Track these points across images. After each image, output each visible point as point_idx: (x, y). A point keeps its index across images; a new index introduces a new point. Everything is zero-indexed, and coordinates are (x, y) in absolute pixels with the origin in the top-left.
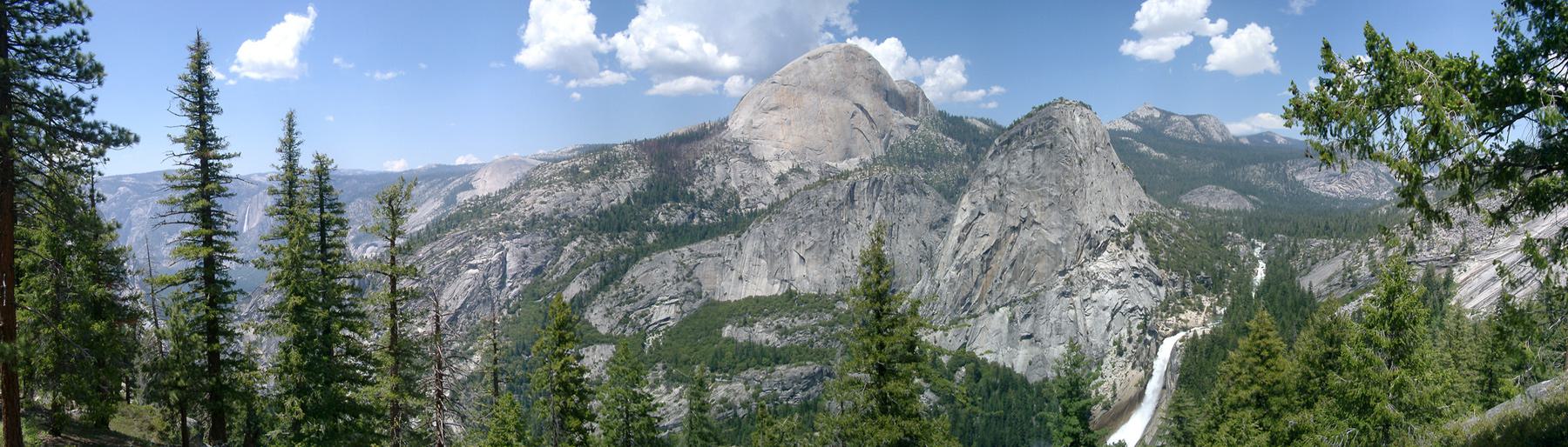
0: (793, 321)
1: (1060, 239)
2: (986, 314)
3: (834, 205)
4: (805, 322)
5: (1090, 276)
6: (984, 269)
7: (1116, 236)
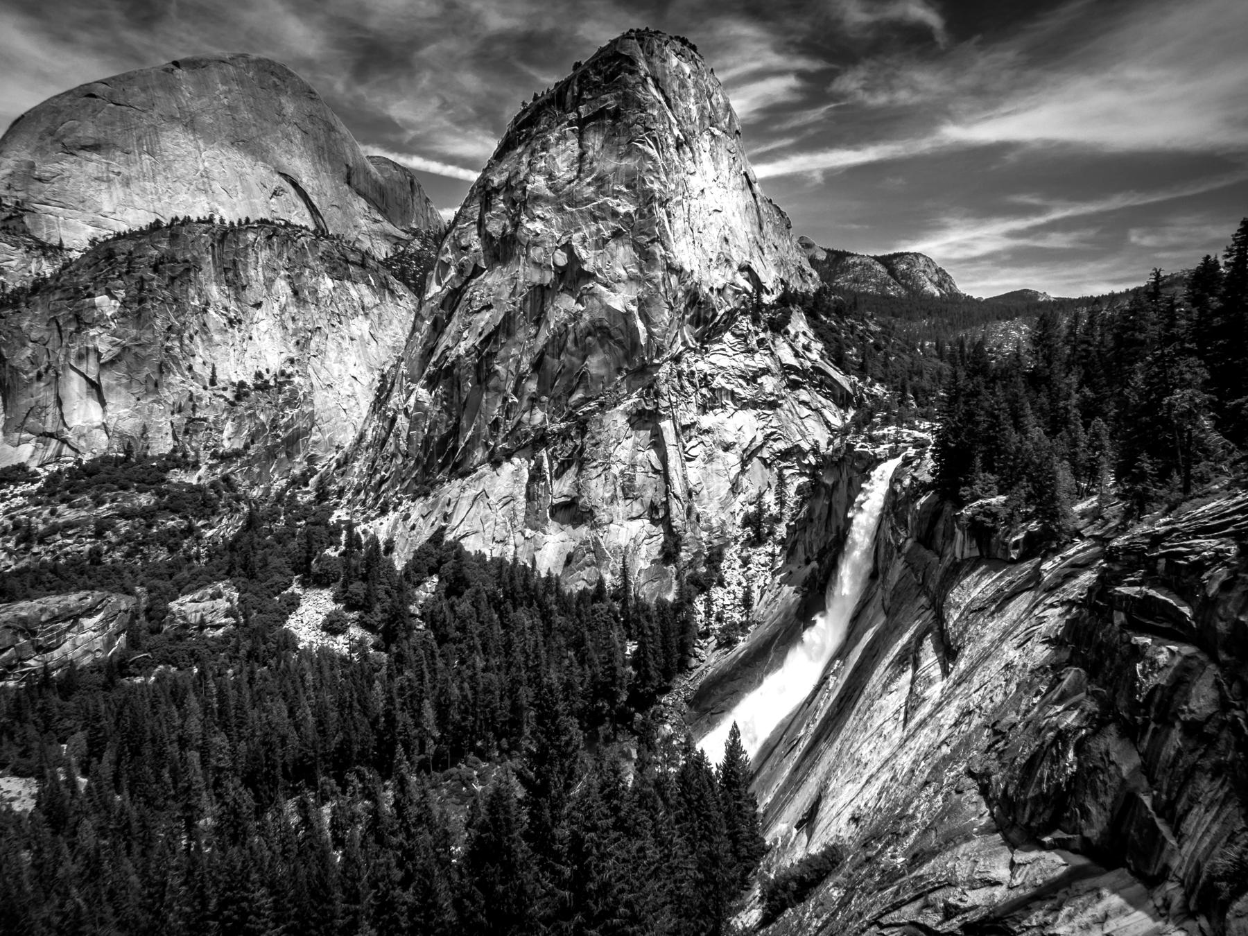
0: (53, 513)
1: (633, 302)
2: (486, 469)
3: (171, 269)
4: (83, 513)
5: (696, 381)
7: (755, 310)
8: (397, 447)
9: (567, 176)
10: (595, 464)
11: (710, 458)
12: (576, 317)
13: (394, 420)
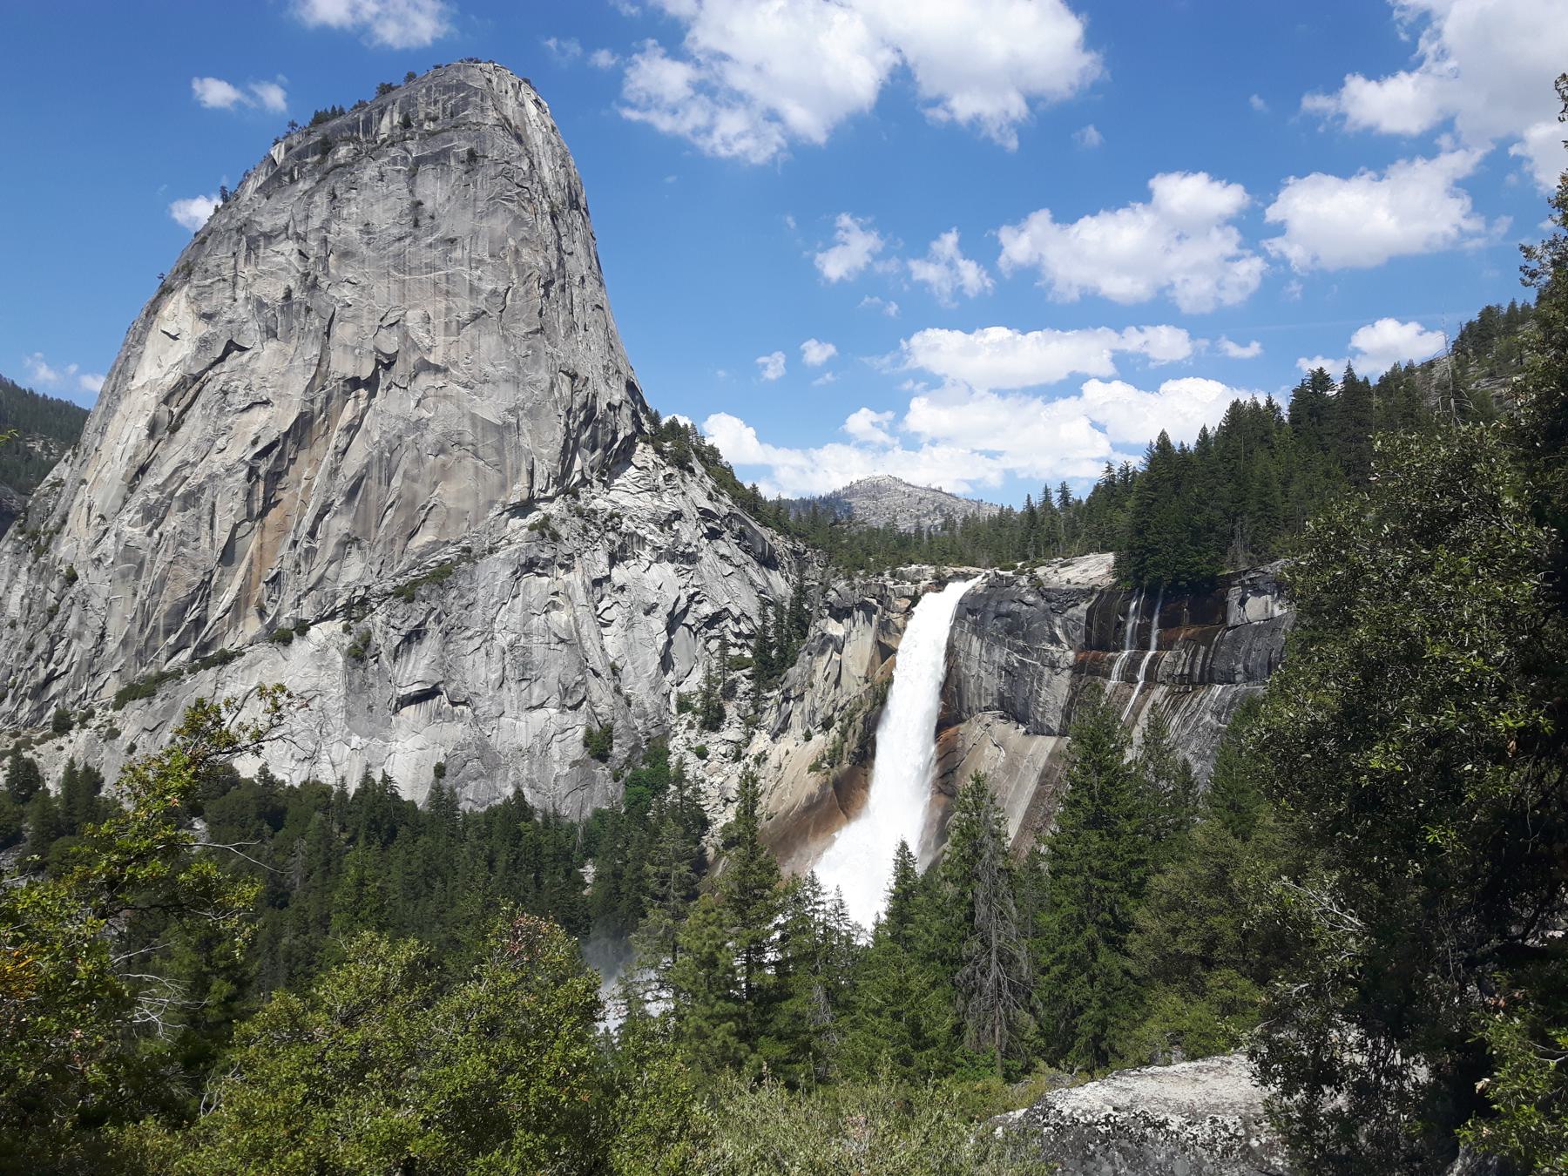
2: (262, 649)
6: (258, 506)
8: (81, 622)
9: (395, 231)
10: (469, 633)
11: (630, 625)
12: (419, 426)
13: (72, 578)
